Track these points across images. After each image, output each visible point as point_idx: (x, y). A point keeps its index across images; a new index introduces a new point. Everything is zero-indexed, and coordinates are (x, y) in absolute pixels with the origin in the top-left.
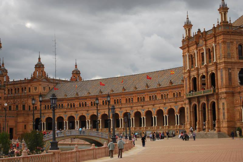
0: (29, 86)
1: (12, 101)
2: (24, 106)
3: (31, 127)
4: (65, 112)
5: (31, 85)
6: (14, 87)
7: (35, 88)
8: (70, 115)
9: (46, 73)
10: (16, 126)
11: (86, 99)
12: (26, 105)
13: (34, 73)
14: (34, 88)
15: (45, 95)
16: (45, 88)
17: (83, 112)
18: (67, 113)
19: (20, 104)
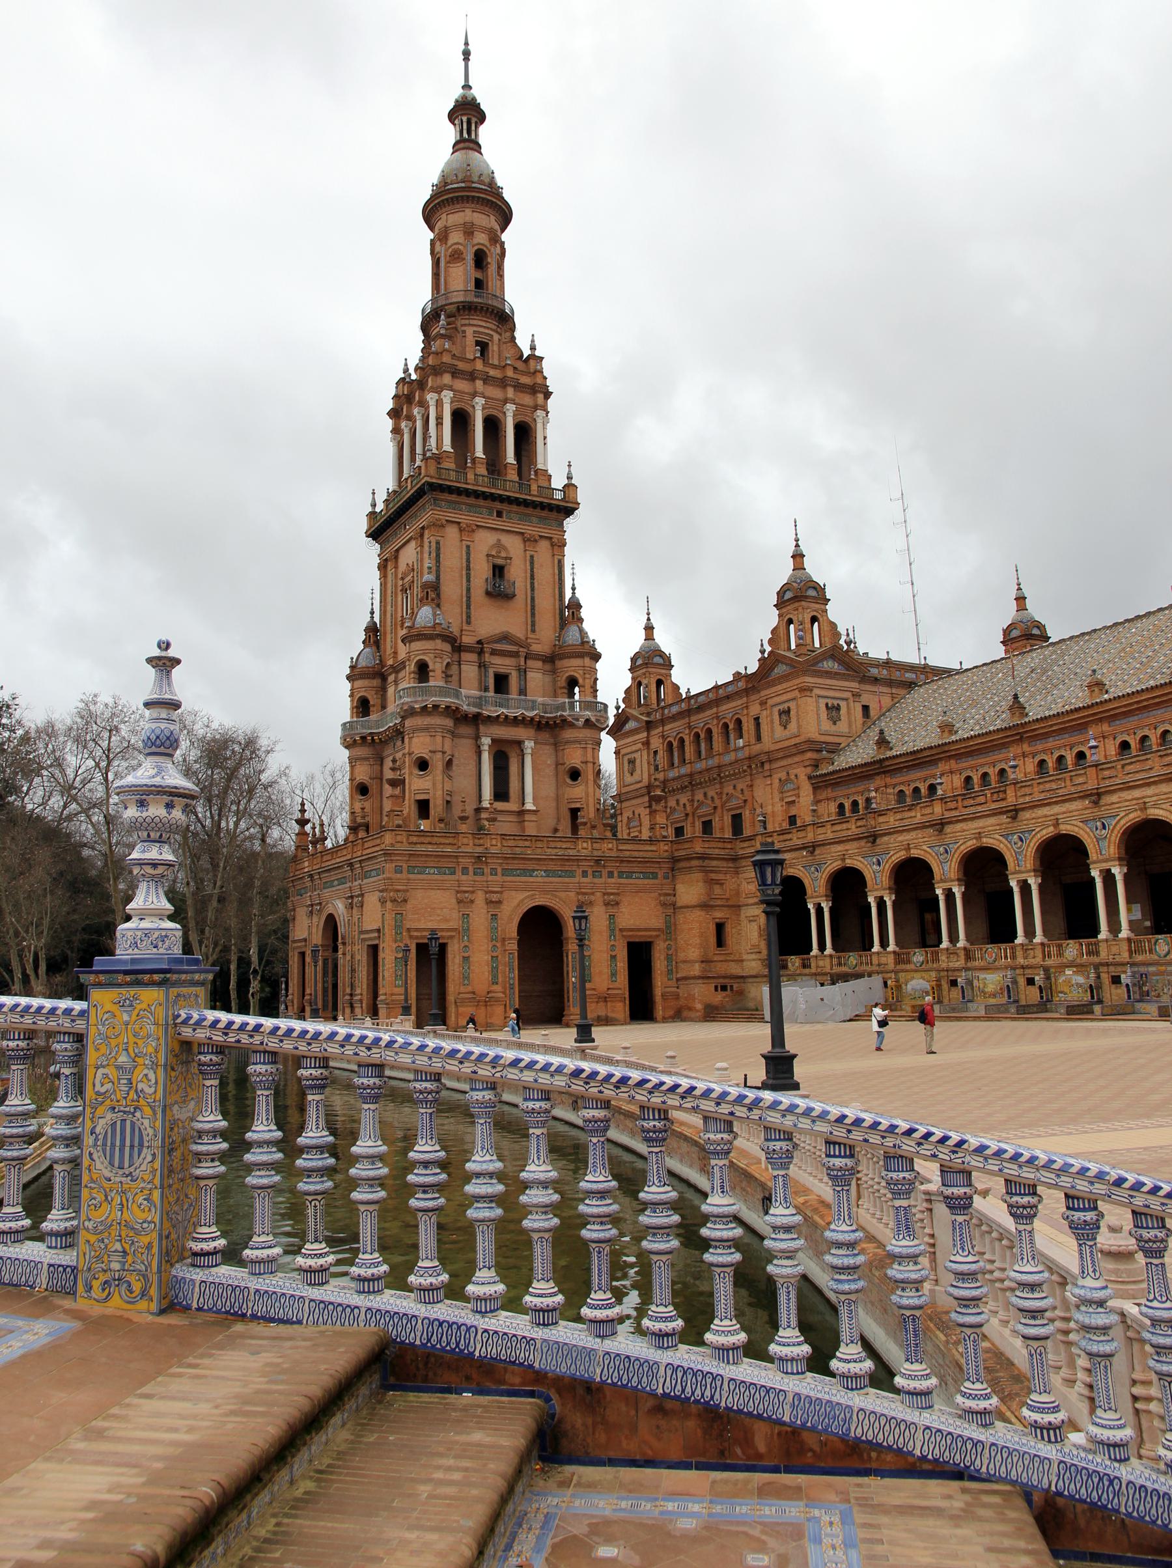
0: (755, 709)
1: (684, 799)
2: (737, 820)
3: (756, 934)
4: (940, 826)
5: (763, 703)
6: (689, 727)
7: (780, 714)
8: (972, 844)
9: (841, 629)
10: (669, 930)
11: (1082, 727)
12: (747, 815)
13: (777, 637)
14: (776, 717)
15: (835, 749)
16: (838, 708)
17: (1056, 809)
18: (948, 829)
19: (719, 810)
